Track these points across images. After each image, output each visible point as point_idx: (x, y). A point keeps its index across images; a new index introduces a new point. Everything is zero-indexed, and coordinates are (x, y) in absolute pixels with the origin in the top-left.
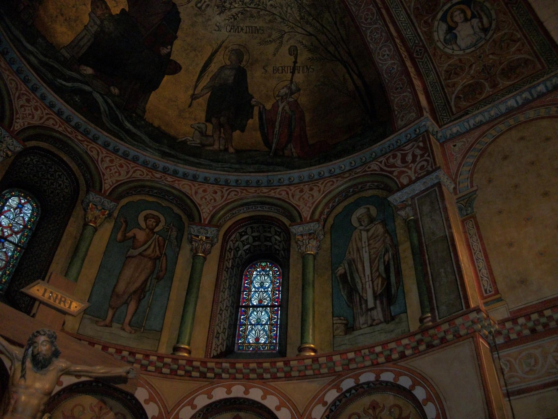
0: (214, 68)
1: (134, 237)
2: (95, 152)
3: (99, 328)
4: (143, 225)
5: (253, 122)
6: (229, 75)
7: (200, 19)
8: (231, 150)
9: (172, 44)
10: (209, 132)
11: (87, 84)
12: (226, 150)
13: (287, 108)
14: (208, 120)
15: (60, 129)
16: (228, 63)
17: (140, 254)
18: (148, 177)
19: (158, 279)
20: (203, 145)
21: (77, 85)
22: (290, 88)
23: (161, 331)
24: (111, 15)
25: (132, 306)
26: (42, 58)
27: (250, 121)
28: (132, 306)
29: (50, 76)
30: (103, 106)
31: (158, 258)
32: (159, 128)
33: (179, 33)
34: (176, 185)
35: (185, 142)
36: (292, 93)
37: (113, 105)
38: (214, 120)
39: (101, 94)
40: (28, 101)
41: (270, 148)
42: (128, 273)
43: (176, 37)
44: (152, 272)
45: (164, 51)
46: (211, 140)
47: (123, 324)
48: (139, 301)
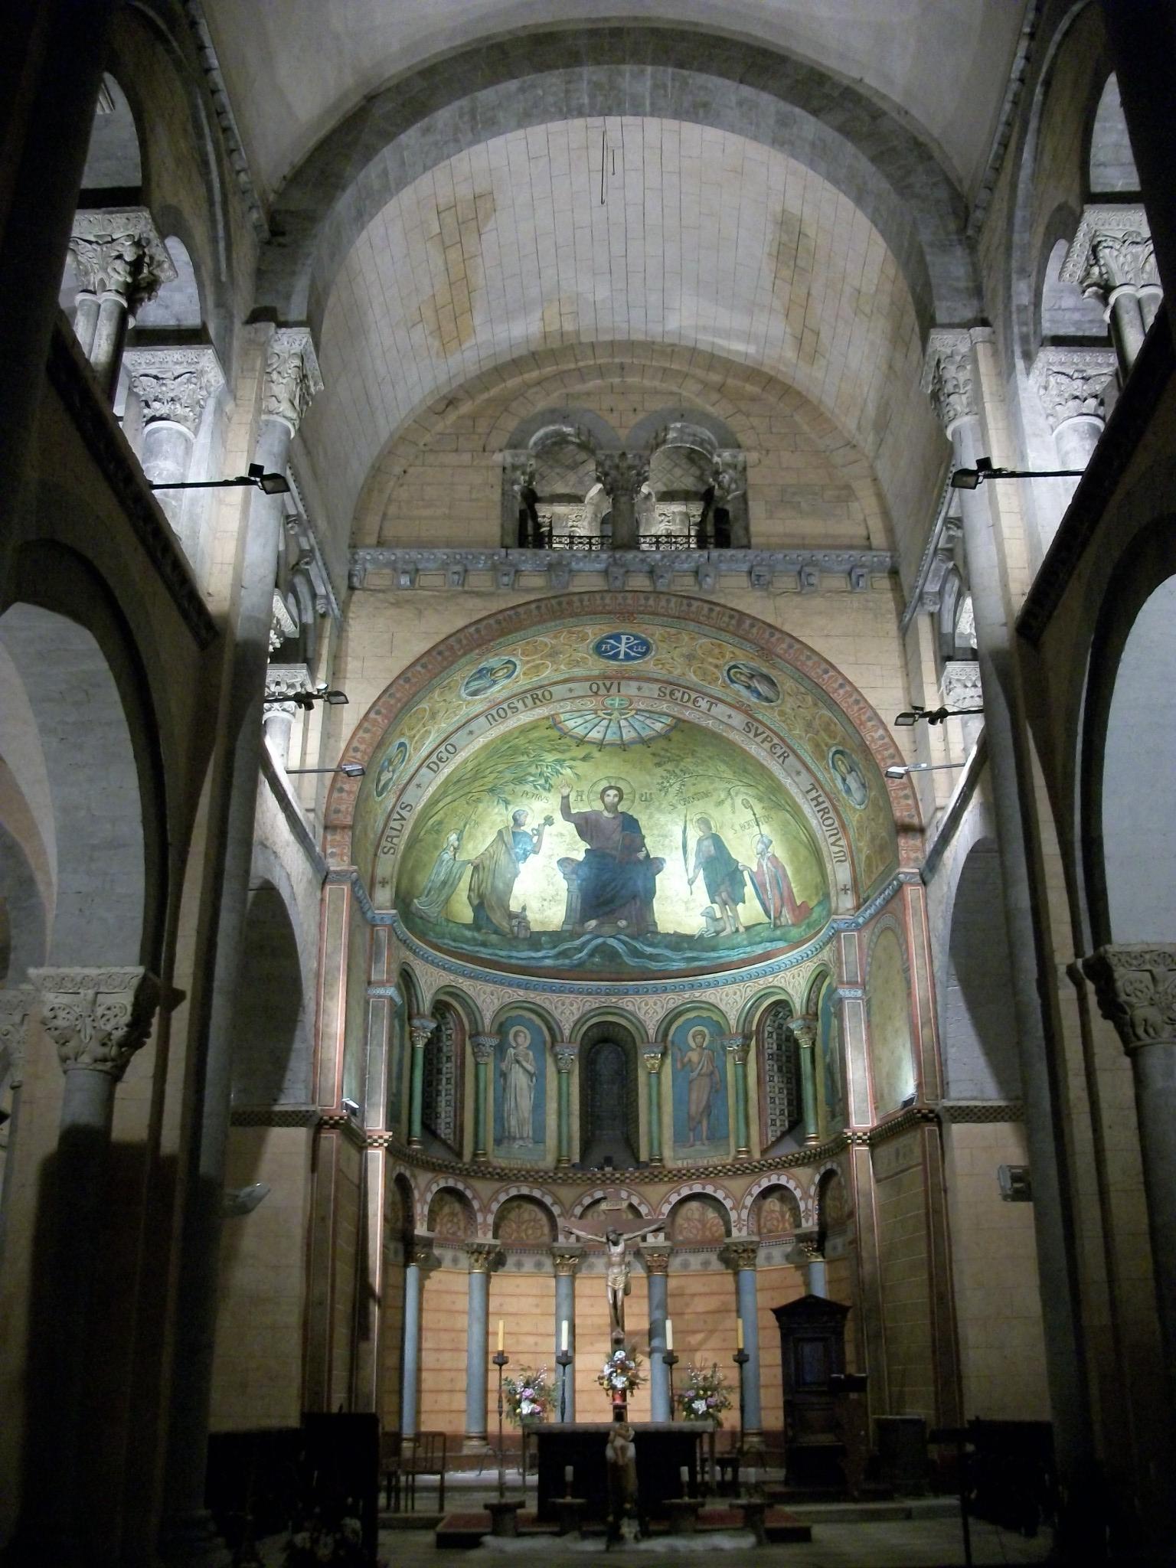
0: (692, 845)
1: (690, 1061)
2: (630, 1004)
3: (685, 1150)
4: (693, 1045)
5: (749, 890)
6: (709, 846)
7: (652, 809)
8: (742, 929)
9: (644, 846)
10: (718, 915)
11: (598, 937)
12: (737, 930)
13: (769, 864)
14: (713, 901)
15: (597, 1005)
16: (701, 834)
17: (699, 1074)
18: (680, 1002)
19: (717, 1091)
20: (718, 933)
21: (590, 946)
22: (763, 842)
23: (728, 1137)
24: (580, 864)
25: (705, 1123)
26: (553, 952)
27: (746, 890)
28: (705, 1123)
29: (567, 961)
30: (620, 948)
31: (712, 1073)
32: (676, 934)
33: (644, 832)
34: (704, 999)
35: (701, 937)
36: (767, 847)
37: (627, 939)
38: (717, 899)
39: (613, 937)
40: (563, 1005)
41: (770, 918)
42: (694, 1096)
43: (644, 837)
44: (712, 1087)
45: (641, 855)
46: (722, 923)
47: (701, 1140)
48: (709, 1115)
